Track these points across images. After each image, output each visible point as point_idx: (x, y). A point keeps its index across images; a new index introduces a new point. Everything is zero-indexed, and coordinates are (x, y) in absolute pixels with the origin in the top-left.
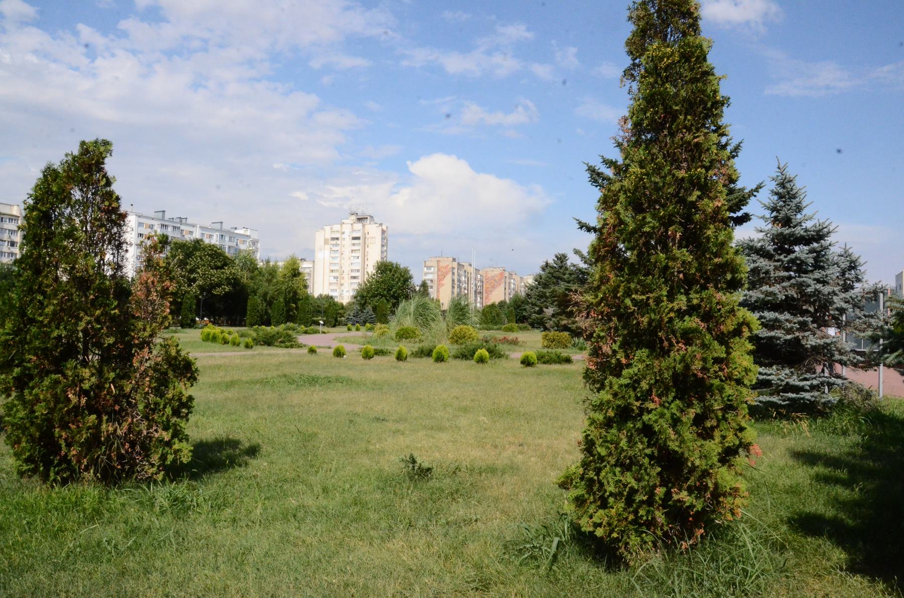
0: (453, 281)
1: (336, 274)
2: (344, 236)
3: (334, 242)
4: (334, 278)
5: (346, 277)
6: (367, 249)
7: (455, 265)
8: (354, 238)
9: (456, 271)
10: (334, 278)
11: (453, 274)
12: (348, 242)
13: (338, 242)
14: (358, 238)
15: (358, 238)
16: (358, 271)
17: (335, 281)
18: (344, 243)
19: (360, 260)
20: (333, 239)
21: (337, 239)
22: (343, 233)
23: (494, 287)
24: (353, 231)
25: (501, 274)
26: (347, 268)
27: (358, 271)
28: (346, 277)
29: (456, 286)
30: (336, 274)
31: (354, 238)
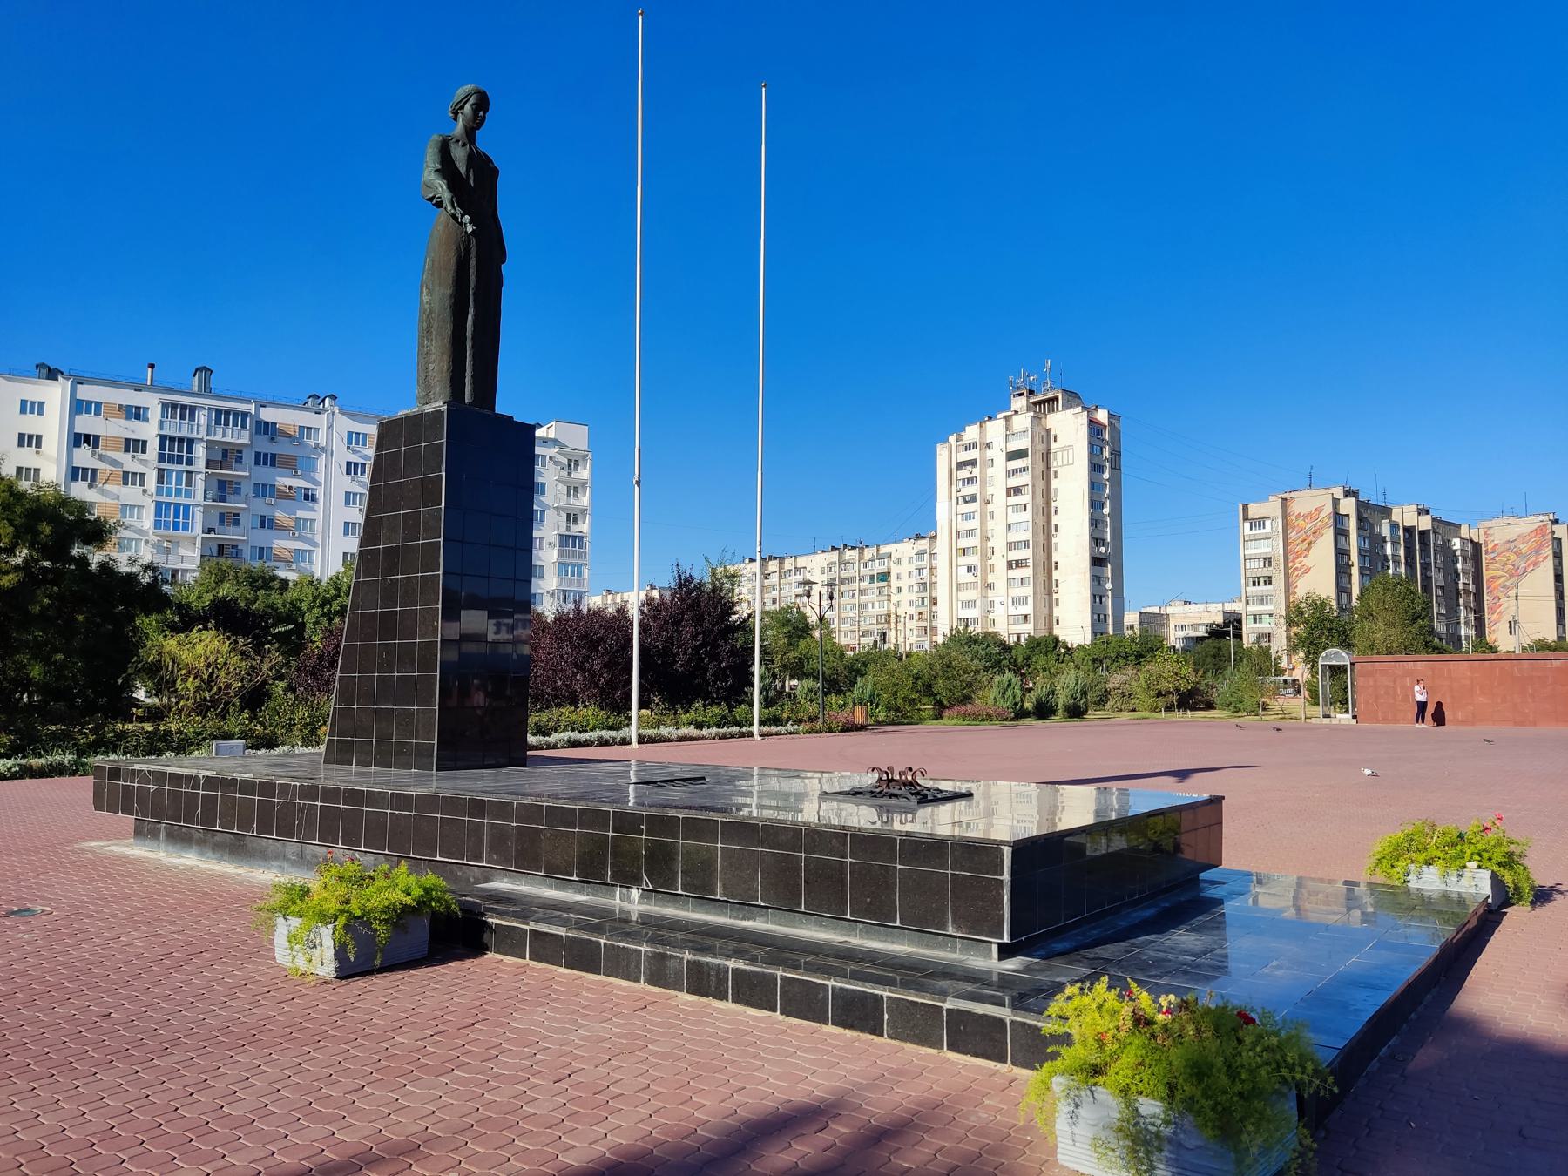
0: (1341, 553)
1: (973, 559)
2: (989, 454)
3: (964, 474)
5: (999, 562)
6: (1055, 483)
7: (1348, 506)
9: (1352, 525)
10: (969, 569)
11: (1340, 533)
13: (976, 472)
14: (1021, 454)
15: (1021, 454)
16: (1026, 544)
17: (969, 578)
18: (990, 471)
20: (961, 465)
21: (973, 463)
22: (989, 446)
23: (1518, 574)
24: (1009, 434)
25: (1539, 532)
27: (1026, 544)
28: (999, 562)
29: (1355, 571)
30: (973, 559)
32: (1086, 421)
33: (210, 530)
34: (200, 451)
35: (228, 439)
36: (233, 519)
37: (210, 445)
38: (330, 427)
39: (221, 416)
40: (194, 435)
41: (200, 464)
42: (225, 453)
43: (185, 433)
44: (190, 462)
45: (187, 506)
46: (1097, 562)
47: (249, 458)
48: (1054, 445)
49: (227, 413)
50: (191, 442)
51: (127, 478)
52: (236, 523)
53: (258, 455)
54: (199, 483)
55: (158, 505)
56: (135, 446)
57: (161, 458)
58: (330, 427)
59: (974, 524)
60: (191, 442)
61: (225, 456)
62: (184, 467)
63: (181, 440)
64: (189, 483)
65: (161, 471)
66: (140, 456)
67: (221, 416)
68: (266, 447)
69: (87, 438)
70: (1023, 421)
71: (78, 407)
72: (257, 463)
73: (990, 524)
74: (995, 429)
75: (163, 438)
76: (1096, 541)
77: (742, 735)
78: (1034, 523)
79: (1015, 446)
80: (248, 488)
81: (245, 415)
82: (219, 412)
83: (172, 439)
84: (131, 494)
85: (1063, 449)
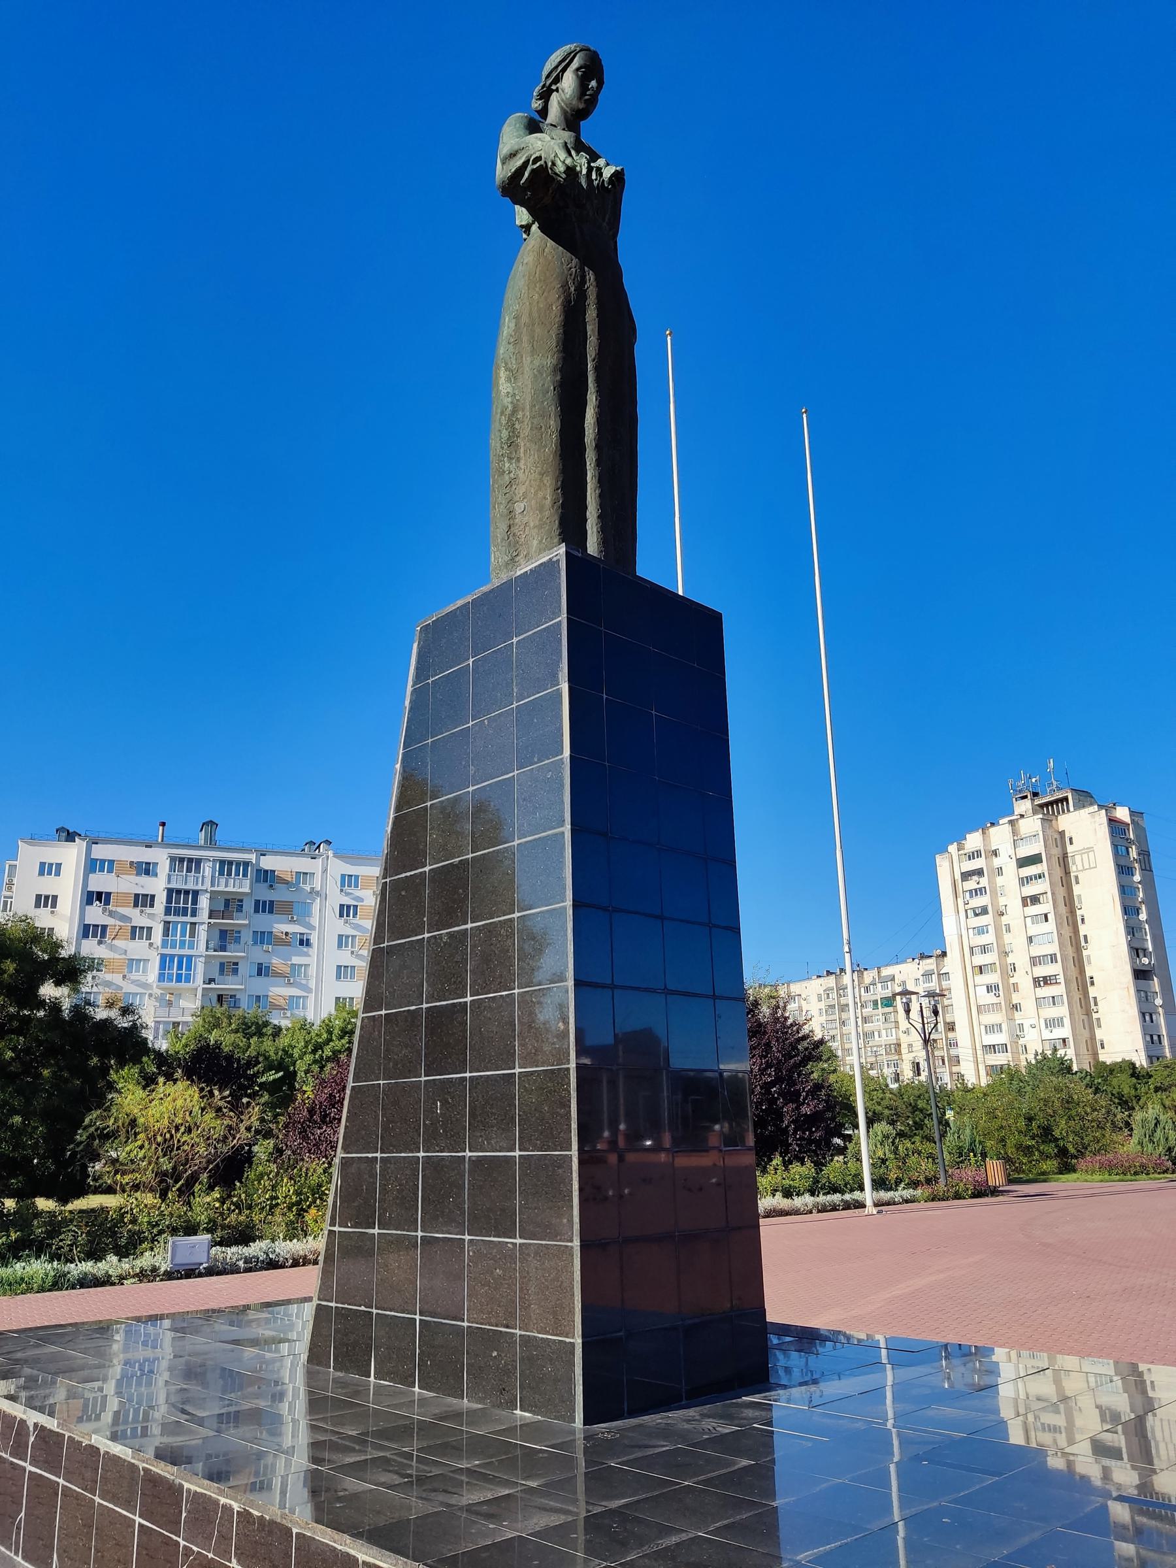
1: (992, 978)
2: (997, 862)
3: (971, 884)
4: (989, 989)
5: (1023, 979)
6: (1077, 890)
8: (1024, 862)
10: (989, 989)
12: (1011, 872)
13: (984, 882)
14: (1035, 859)
15: (1035, 859)
16: (1053, 958)
17: (990, 999)
18: (1000, 880)
19: (1051, 926)
20: (966, 876)
21: (979, 872)
22: (995, 853)
24: (1017, 838)
26: (1020, 957)
27: (1053, 958)
28: (1023, 979)
30: (992, 978)
31: (1024, 862)
32: (1105, 820)
33: (211, 981)
34: (204, 902)
35: (230, 889)
36: (231, 968)
37: (214, 896)
38: (325, 871)
39: (225, 867)
40: (199, 887)
41: (203, 916)
42: (227, 903)
43: (190, 886)
44: (194, 914)
45: (190, 958)
46: (1141, 975)
47: (248, 906)
48: (1070, 849)
49: (230, 863)
50: (196, 893)
51: (136, 932)
52: (235, 972)
53: (257, 902)
54: (202, 933)
55: (163, 957)
56: (144, 901)
57: (168, 911)
58: (325, 871)
59: (989, 938)
60: (196, 893)
61: (228, 905)
62: (189, 919)
63: (187, 892)
64: (192, 935)
65: (167, 923)
66: (148, 910)
67: (225, 867)
68: (266, 895)
69: (99, 894)
70: (1032, 824)
71: (92, 865)
72: (256, 911)
73: (1007, 938)
74: (1000, 835)
75: (170, 891)
76: (1136, 951)
77: (847, 1206)
78: (1060, 935)
79: (1026, 851)
80: (247, 937)
81: (246, 864)
82: (222, 862)
83: (179, 892)
84: (137, 949)
85: (1082, 852)
